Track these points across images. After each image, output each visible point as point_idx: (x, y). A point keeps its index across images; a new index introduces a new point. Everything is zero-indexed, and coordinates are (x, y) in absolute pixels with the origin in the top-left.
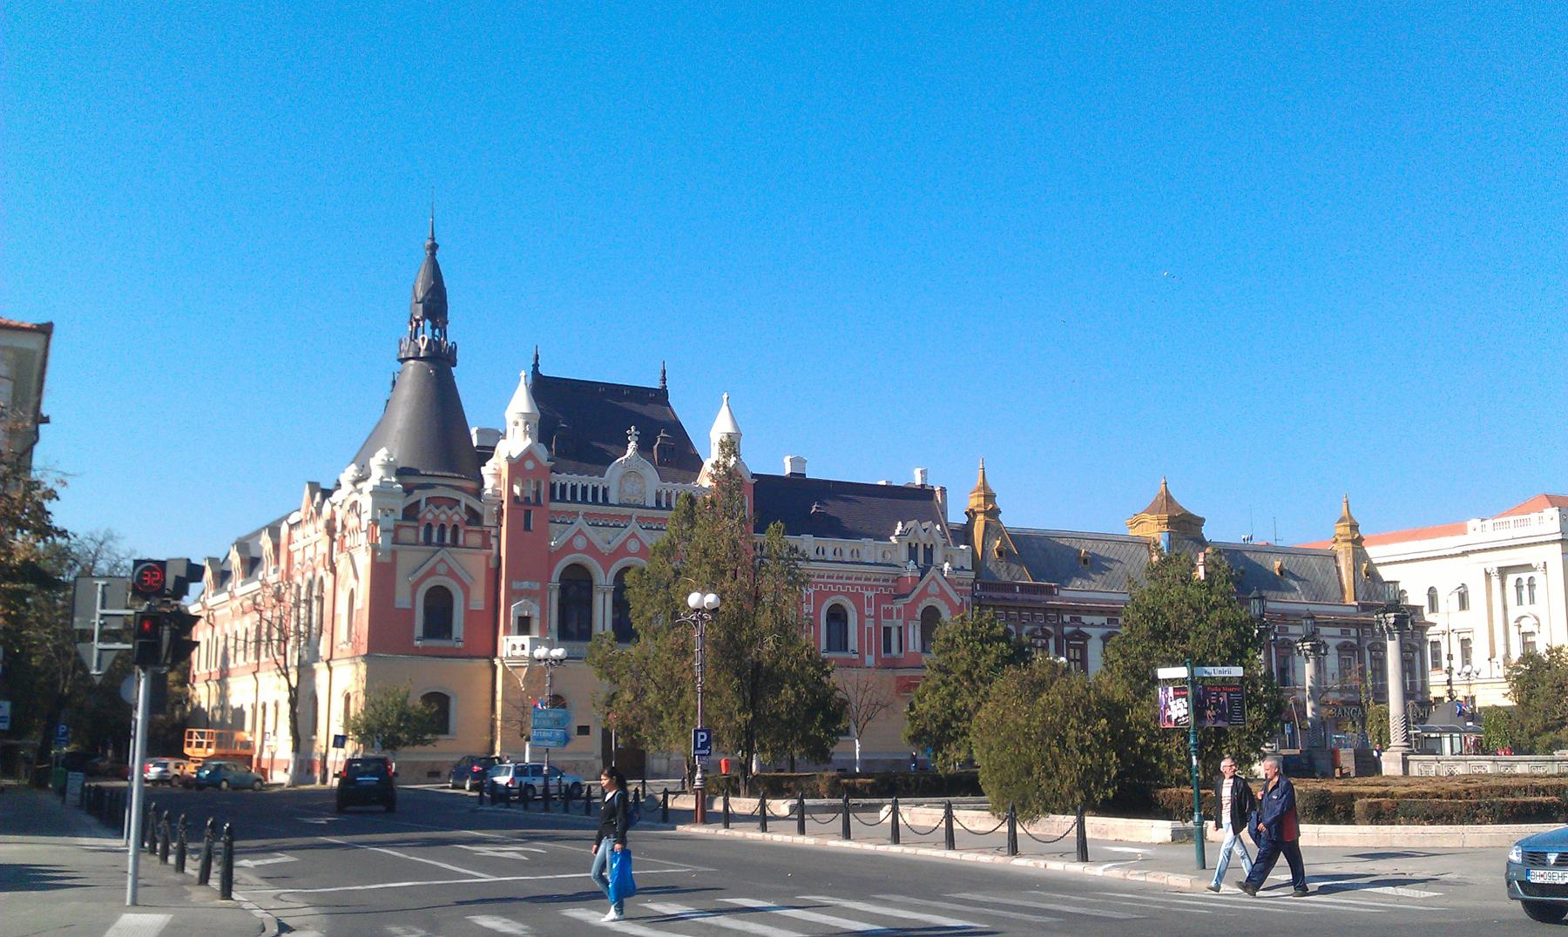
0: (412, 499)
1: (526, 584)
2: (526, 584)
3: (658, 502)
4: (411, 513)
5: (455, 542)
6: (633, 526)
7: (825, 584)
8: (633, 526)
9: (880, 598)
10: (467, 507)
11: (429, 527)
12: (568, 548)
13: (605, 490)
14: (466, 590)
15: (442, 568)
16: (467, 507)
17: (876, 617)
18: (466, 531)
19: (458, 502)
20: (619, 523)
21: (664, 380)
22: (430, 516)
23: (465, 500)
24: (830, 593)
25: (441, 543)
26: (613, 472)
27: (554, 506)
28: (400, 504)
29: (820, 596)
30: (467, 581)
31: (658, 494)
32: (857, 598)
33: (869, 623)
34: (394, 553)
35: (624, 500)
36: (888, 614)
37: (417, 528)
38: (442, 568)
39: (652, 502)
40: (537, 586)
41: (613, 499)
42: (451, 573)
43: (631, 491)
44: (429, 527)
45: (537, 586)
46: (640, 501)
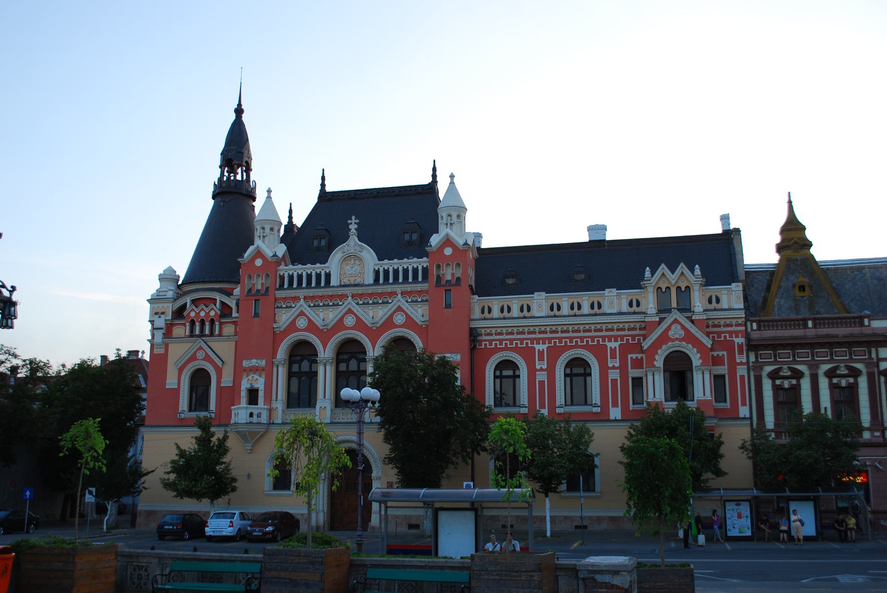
0: (180, 303)
1: (254, 362)
2: (254, 362)
3: (377, 280)
4: (179, 313)
5: (212, 334)
6: (350, 303)
7: (560, 339)
8: (350, 303)
9: (626, 349)
10: (222, 303)
11: (193, 323)
12: (292, 327)
13: (328, 276)
14: (219, 372)
15: (200, 355)
16: (222, 303)
17: (623, 369)
18: (221, 324)
19: (214, 301)
20: (336, 299)
21: (434, 176)
22: (193, 314)
23: (219, 297)
24: (567, 348)
25: (202, 334)
26: (336, 256)
27: (280, 294)
28: (169, 309)
29: (554, 353)
30: (219, 363)
31: (377, 273)
32: (600, 352)
33: (614, 375)
34: (167, 346)
35: (346, 281)
36: (638, 364)
37: (184, 325)
38: (200, 355)
39: (371, 281)
40: (263, 363)
41: (334, 282)
42: (207, 358)
43: (351, 272)
44: (193, 323)
45: (263, 363)
46: (359, 280)
